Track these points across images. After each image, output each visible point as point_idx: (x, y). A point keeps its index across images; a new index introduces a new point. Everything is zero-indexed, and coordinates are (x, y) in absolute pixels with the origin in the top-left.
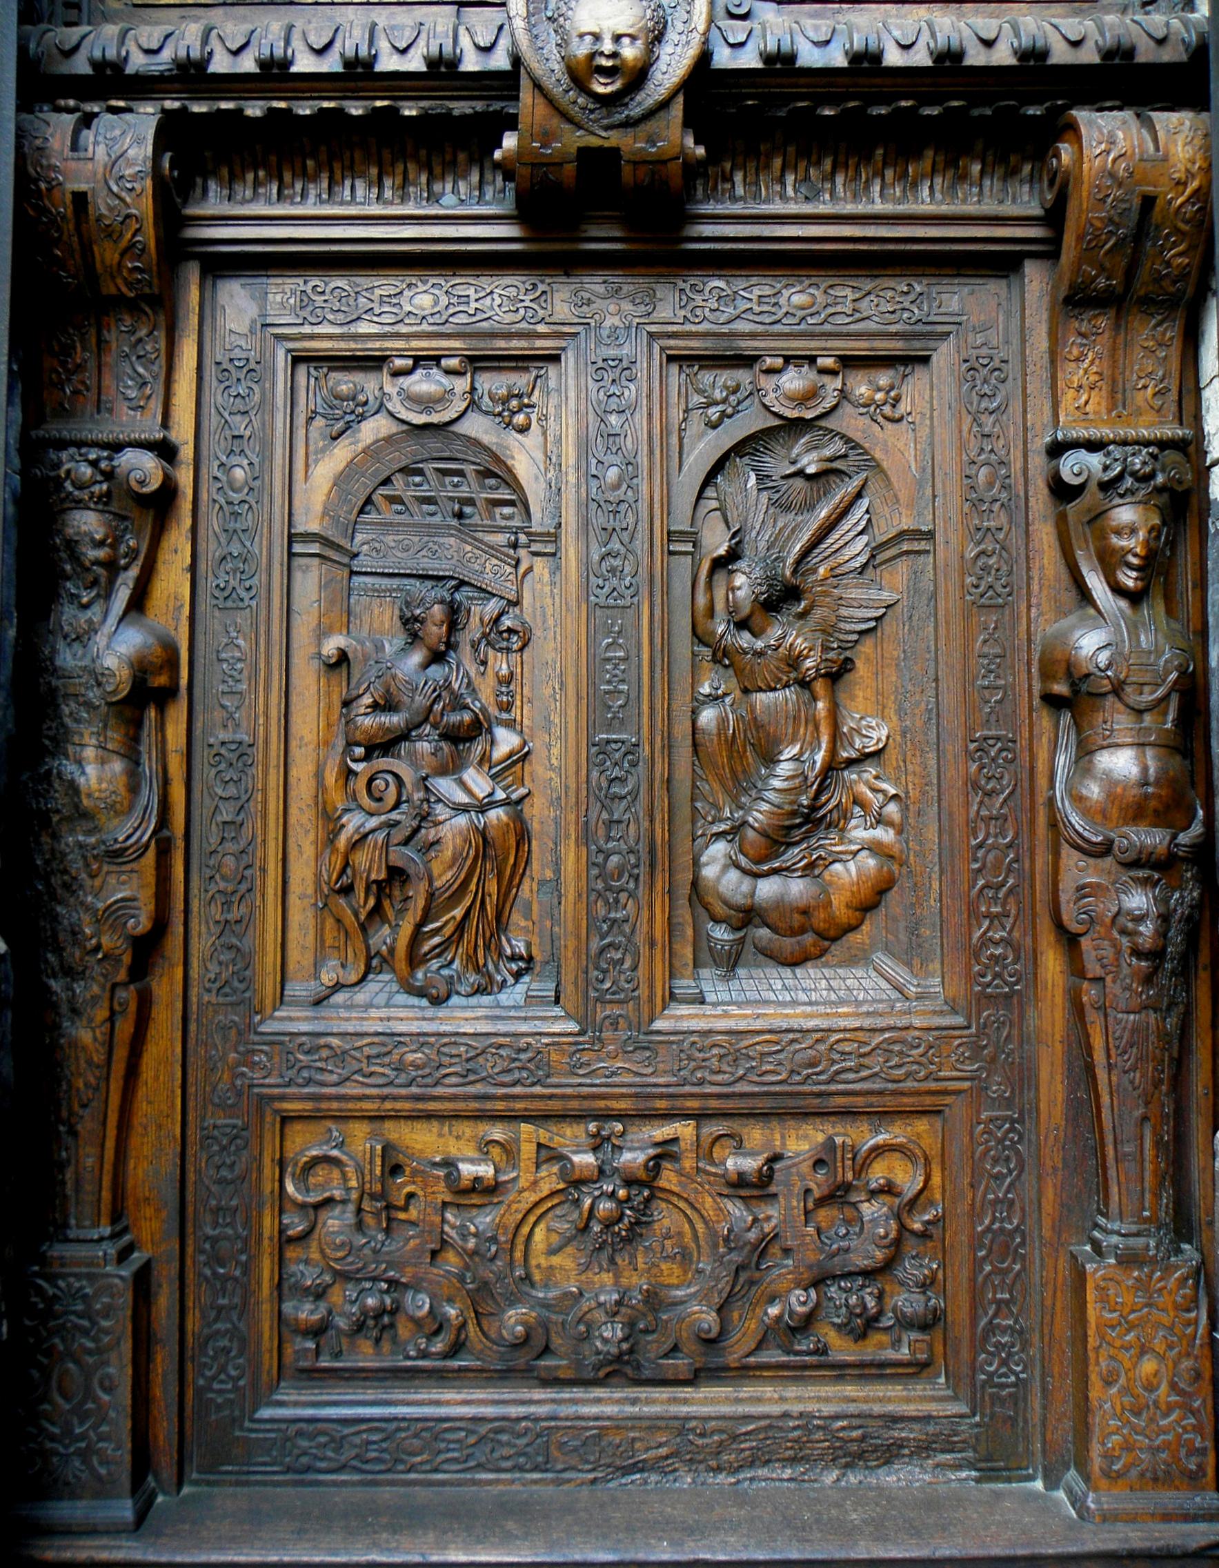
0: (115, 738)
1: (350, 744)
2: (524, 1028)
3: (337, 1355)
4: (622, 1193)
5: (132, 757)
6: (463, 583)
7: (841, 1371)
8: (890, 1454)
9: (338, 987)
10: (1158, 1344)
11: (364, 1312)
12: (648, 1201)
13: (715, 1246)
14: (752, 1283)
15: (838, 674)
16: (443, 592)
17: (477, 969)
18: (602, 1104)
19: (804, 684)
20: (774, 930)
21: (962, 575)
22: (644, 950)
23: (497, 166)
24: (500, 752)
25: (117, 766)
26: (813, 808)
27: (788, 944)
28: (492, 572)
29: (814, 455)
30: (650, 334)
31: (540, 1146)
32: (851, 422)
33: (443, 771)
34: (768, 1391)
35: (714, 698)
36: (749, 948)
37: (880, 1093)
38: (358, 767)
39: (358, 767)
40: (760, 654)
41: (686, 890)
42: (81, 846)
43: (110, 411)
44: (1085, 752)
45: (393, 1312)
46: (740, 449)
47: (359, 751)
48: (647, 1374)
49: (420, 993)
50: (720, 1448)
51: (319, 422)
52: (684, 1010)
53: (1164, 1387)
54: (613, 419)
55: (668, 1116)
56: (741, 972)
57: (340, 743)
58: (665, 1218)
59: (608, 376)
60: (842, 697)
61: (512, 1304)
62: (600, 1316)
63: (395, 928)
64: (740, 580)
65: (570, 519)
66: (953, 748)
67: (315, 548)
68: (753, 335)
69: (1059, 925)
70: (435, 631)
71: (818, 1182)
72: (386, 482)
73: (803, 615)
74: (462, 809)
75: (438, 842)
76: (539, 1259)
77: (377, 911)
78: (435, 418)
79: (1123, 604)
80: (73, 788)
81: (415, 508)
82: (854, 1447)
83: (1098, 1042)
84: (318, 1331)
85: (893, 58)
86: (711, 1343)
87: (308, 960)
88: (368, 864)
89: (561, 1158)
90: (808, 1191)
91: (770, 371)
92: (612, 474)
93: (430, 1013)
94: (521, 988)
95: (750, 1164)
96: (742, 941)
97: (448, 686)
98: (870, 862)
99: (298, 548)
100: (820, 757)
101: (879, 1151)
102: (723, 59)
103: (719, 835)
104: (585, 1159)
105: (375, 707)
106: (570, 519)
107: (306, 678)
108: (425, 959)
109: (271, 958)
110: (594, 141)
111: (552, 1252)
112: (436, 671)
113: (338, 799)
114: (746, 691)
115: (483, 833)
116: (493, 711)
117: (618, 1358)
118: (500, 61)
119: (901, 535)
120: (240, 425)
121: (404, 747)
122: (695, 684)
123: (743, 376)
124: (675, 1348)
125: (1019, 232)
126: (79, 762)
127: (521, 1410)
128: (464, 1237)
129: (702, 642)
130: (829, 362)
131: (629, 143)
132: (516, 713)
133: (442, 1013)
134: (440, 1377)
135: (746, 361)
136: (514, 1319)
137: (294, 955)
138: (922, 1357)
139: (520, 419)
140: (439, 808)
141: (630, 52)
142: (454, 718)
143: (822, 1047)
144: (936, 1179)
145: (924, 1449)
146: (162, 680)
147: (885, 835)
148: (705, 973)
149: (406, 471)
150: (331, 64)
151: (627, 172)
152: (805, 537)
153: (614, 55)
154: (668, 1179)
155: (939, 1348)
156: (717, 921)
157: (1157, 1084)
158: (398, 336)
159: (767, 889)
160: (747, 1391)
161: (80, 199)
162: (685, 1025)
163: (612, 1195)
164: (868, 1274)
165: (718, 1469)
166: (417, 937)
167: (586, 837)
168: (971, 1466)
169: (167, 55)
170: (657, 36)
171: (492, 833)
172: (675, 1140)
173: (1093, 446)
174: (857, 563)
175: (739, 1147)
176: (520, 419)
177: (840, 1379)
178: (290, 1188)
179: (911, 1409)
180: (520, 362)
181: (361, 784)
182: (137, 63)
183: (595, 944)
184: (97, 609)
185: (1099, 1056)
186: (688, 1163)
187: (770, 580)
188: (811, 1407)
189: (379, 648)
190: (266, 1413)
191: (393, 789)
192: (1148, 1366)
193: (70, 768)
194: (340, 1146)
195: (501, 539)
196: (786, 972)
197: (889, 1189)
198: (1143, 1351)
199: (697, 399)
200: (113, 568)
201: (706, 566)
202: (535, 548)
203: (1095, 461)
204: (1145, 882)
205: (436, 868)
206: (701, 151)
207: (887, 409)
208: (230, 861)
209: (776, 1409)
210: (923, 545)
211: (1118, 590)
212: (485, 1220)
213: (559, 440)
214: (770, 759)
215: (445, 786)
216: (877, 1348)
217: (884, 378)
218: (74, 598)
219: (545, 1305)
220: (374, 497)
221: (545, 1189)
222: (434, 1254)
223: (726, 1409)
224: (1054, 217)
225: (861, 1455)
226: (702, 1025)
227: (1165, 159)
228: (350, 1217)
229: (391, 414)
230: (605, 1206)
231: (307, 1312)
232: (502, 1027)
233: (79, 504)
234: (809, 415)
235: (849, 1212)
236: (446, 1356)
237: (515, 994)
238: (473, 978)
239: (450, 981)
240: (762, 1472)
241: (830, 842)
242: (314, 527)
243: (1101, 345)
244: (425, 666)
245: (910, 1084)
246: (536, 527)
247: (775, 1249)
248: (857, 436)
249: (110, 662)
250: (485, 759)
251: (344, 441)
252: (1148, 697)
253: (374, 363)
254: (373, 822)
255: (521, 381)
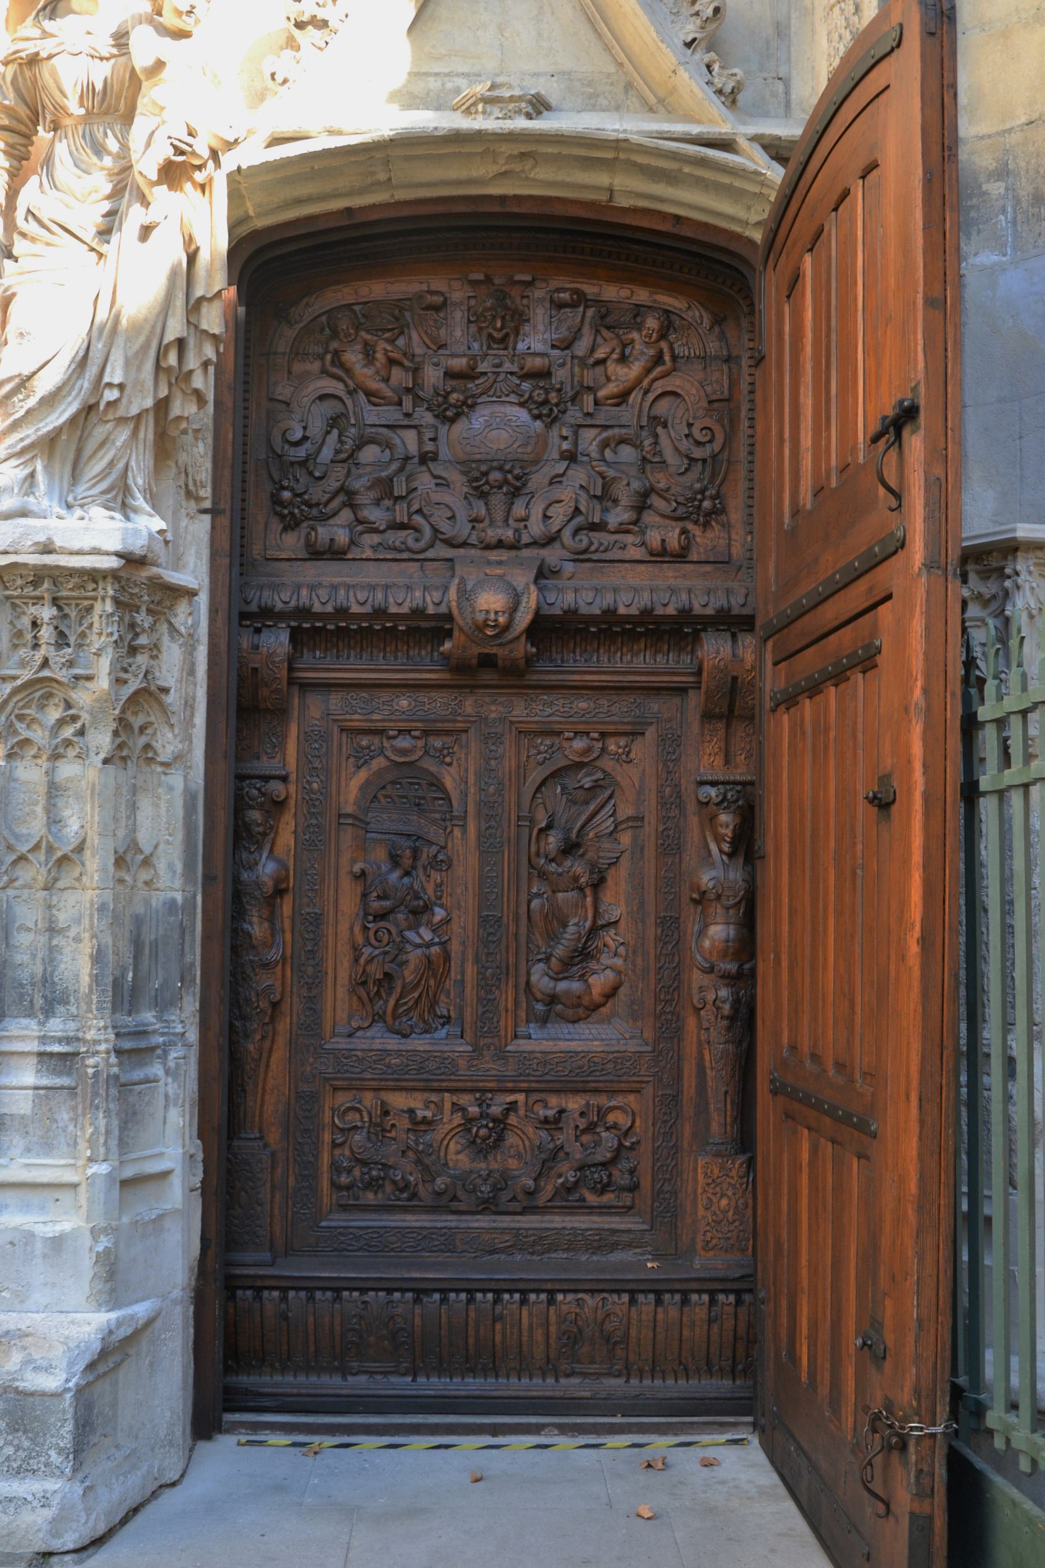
0: (265, 913)
1: (366, 914)
2: (446, 1048)
3: (357, 1199)
4: (491, 1125)
5: (271, 920)
6: (419, 837)
7: (591, 1210)
8: (614, 1247)
9: (360, 1028)
10: (730, 1193)
11: (372, 1178)
12: (503, 1129)
13: (532, 1150)
14: (551, 1168)
15: (598, 884)
16: (409, 843)
17: (425, 1022)
18: (481, 1084)
19: (581, 889)
20: (565, 1005)
21: (657, 838)
22: (503, 1014)
23: (442, 654)
24: (437, 918)
25: (266, 925)
26: (584, 948)
27: (570, 1012)
28: (433, 832)
29: (588, 779)
30: (511, 722)
31: (453, 1104)
32: (607, 763)
33: (410, 928)
34: (557, 1218)
35: (538, 895)
36: (553, 1014)
37: (611, 1081)
38: (370, 926)
39: (370, 926)
40: (560, 875)
41: (523, 986)
42: (251, 961)
43: (258, 758)
44: (706, 926)
45: (384, 1179)
46: (554, 775)
47: (371, 918)
48: (501, 1209)
49: (398, 1033)
50: (534, 1243)
51: (352, 760)
52: (522, 1042)
53: (731, 1213)
54: (493, 762)
55: (513, 1091)
56: (549, 1025)
57: (362, 913)
58: (511, 1139)
59: (490, 742)
60: (601, 895)
61: (439, 1176)
62: (479, 1181)
63: (386, 1002)
64: (551, 839)
65: (471, 808)
66: (651, 920)
67: (350, 821)
68: (560, 723)
69: (694, 1007)
70: (407, 862)
71: (582, 1123)
72: (384, 788)
73: (582, 856)
74: (418, 946)
75: (407, 961)
76: (451, 1156)
77: (378, 993)
78: (407, 759)
79: (725, 857)
80: (250, 935)
81: (397, 800)
82: (595, 1244)
83: (707, 1057)
84: (349, 1187)
85: (622, 610)
86: (530, 1194)
87: (345, 1016)
88: (376, 971)
89: (463, 1109)
90: (577, 1127)
91: (569, 739)
92: (492, 789)
93: (403, 1041)
94: (444, 1031)
95: (550, 1113)
96: (549, 1011)
97: (412, 887)
98: (610, 974)
99: (342, 821)
100: (588, 924)
101: (612, 1109)
102: (547, 611)
103: (540, 960)
104: (474, 1110)
105: (379, 897)
106: (471, 808)
107: (346, 884)
108: (400, 1016)
109: (329, 1015)
110: (486, 651)
111: (458, 1153)
112: (406, 880)
113: (360, 939)
114: (554, 892)
115: (428, 958)
116: (433, 899)
117: (487, 1201)
118: (443, 609)
119: (629, 819)
120: (317, 765)
121: (391, 917)
122: (530, 887)
123: (557, 741)
124: (514, 1199)
125: (684, 679)
126: (251, 923)
127: (443, 1224)
128: (417, 1144)
129: (533, 867)
130: (596, 735)
131: (501, 652)
132: (444, 900)
133: (408, 1041)
134: (405, 1209)
135: (559, 733)
136: (440, 1183)
137: (339, 1013)
138: (628, 1204)
139: (448, 759)
140: (408, 946)
141: (502, 619)
142: (416, 903)
143: (585, 1060)
144: (638, 1123)
145: (629, 1246)
146: (284, 886)
147: (619, 962)
148: (532, 1025)
149: (393, 783)
150: (367, 609)
151: (500, 662)
152: (584, 818)
153: (496, 620)
154: (512, 1120)
155: (637, 1201)
156: (538, 1001)
157: (733, 1076)
158: (391, 720)
159: (562, 986)
160: (547, 1218)
161: (255, 670)
162: (521, 1049)
163: (486, 1126)
164: (603, 1164)
165: (532, 1253)
166: (397, 1006)
167: (477, 960)
168: (650, 1253)
169: (293, 603)
170: (513, 610)
171: (434, 958)
172: (516, 1102)
173: (713, 784)
174: (608, 831)
175: (546, 1107)
176: (448, 759)
177: (590, 1214)
178: (337, 1121)
179: (622, 1227)
180: (448, 733)
181: (371, 934)
182: (279, 606)
183: (480, 1010)
184: (256, 854)
185: (707, 1064)
186: (522, 1112)
187: (566, 839)
188: (577, 1225)
189: (379, 868)
190: (323, 1224)
191: (386, 936)
192: (724, 1202)
193: (246, 926)
194: (360, 1102)
195: (437, 816)
196: (570, 1026)
197: (615, 1126)
198: (722, 1196)
199: (533, 752)
200: (264, 834)
201: (535, 832)
202: (455, 822)
203: (713, 792)
204: (727, 985)
205: (406, 973)
206: (534, 650)
207: (624, 757)
208: (310, 970)
209: (559, 1226)
210: (639, 824)
211: (721, 851)
212: (428, 1137)
213: (467, 771)
214: (565, 925)
215: (410, 935)
216: (608, 1198)
217: (622, 742)
218: (247, 849)
219: (454, 1177)
220: (380, 796)
221: (456, 1123)
222: (404, 1152)
223: (537, 1225)
224: (699, 673)
225: (599, 1248)
226: (529, 1048)
227: (742, 660)
228: (364, 1133)
229: (387, 757)
230: (483, 1132)
231: (344, 1179)
232: (436, 1048)
233: (252, 808)
234: (586, 760)
235: (596, 1138)
236: (409, 1199)
237: (443, 1033)
238: (421, 1025)
239: (411, 1026)
240: (554, 1255)
241: (593, 965)
242: (349, 809)
243: (722, 733)
244: (402, 878)
245: (624, 1078)
246: (455, 814)
247: (561, 1154)
248: (609, 770)
249: (265, 879)
250: (429, 923)
251: (364, 769)
252: (731, 902)
253: (380, 732)
254: (377, 952)
255: (449, 740)
